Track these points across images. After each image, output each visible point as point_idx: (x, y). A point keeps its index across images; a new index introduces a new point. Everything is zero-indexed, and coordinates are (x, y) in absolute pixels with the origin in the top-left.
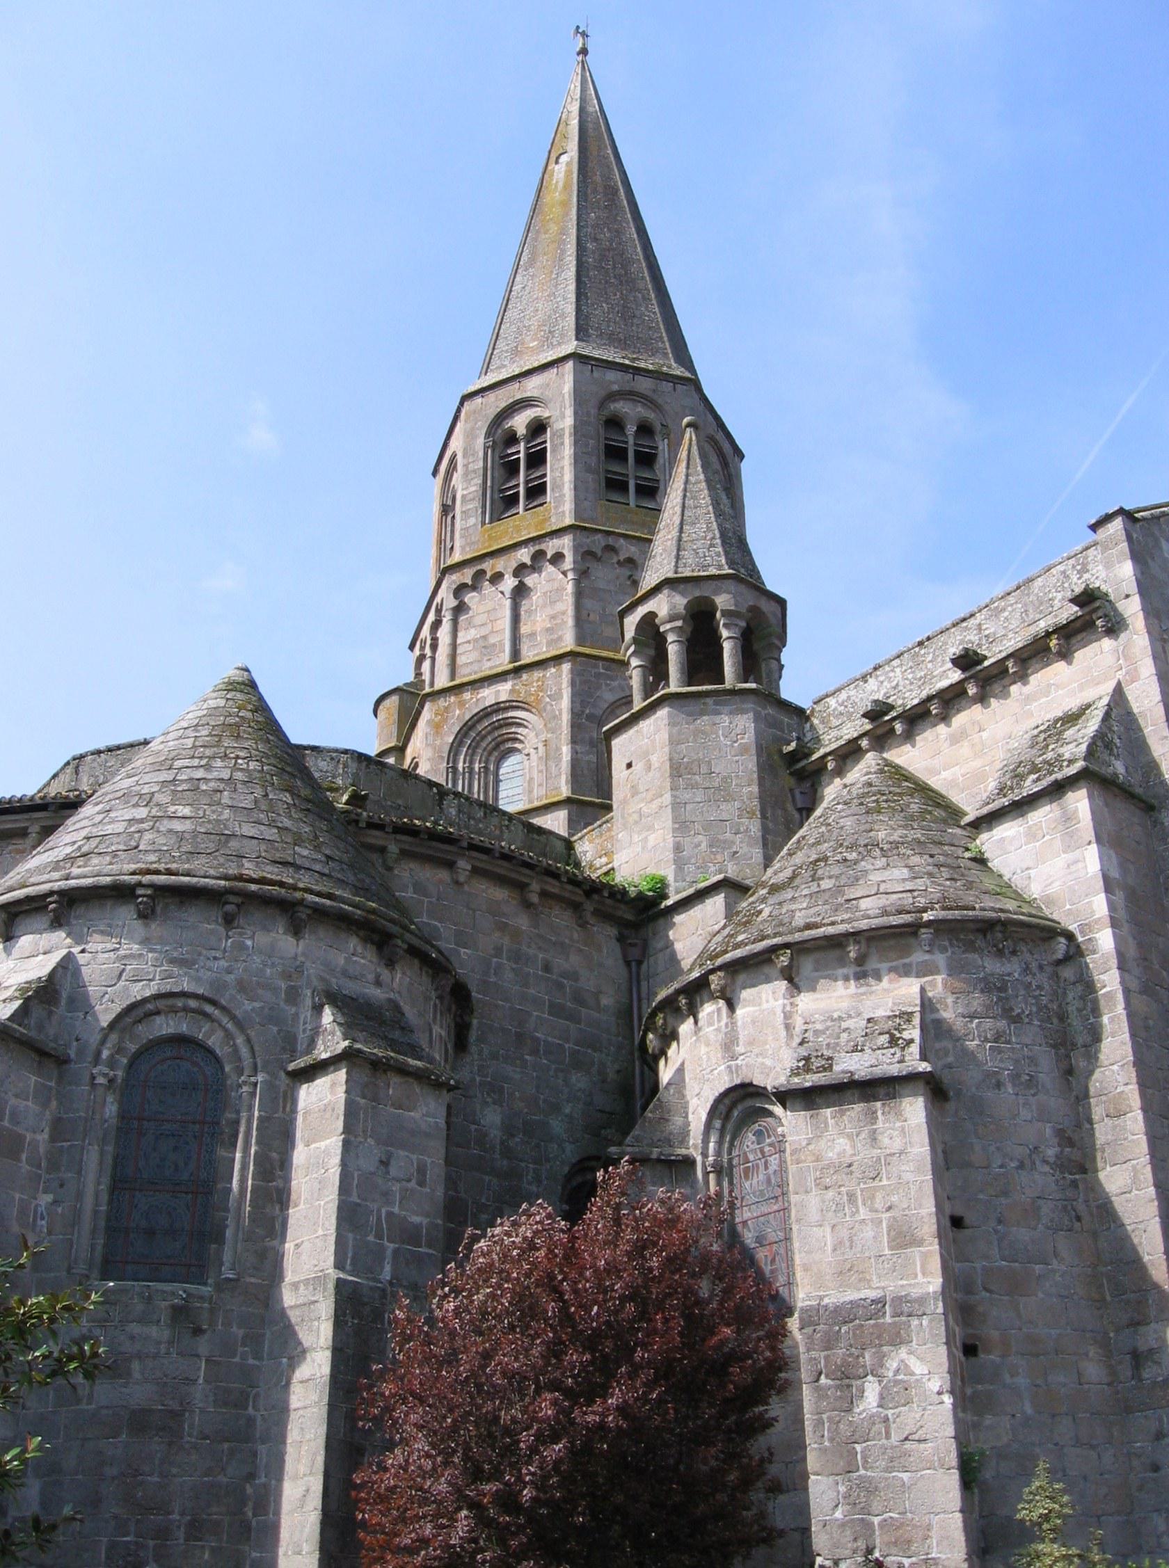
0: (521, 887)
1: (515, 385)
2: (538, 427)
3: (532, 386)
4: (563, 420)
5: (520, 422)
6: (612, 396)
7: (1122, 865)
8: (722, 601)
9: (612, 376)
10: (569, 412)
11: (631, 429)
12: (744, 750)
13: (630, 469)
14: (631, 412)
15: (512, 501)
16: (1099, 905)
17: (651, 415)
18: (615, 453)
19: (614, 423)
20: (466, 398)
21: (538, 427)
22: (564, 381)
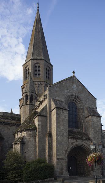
0: (9, 125)
1: (25, 65)
2: (29, 69)
3: (28, 63)
4: (30, 68)
5: (27, 68)
6: (36, 64)
7: (42, 123)
8: (28, 95)
9: (35, 61)
10: (30, 67)
11: (37, 67)
12: (28, 110)
13: (37, 72)
14: (37, 65)
15: (27, 78)
16: (38, 127)
17: (39, 65)
18: (36, 70)
19: (36, 67)
20: (23, 66)
21: (29, 69)
22: (30, 63)
